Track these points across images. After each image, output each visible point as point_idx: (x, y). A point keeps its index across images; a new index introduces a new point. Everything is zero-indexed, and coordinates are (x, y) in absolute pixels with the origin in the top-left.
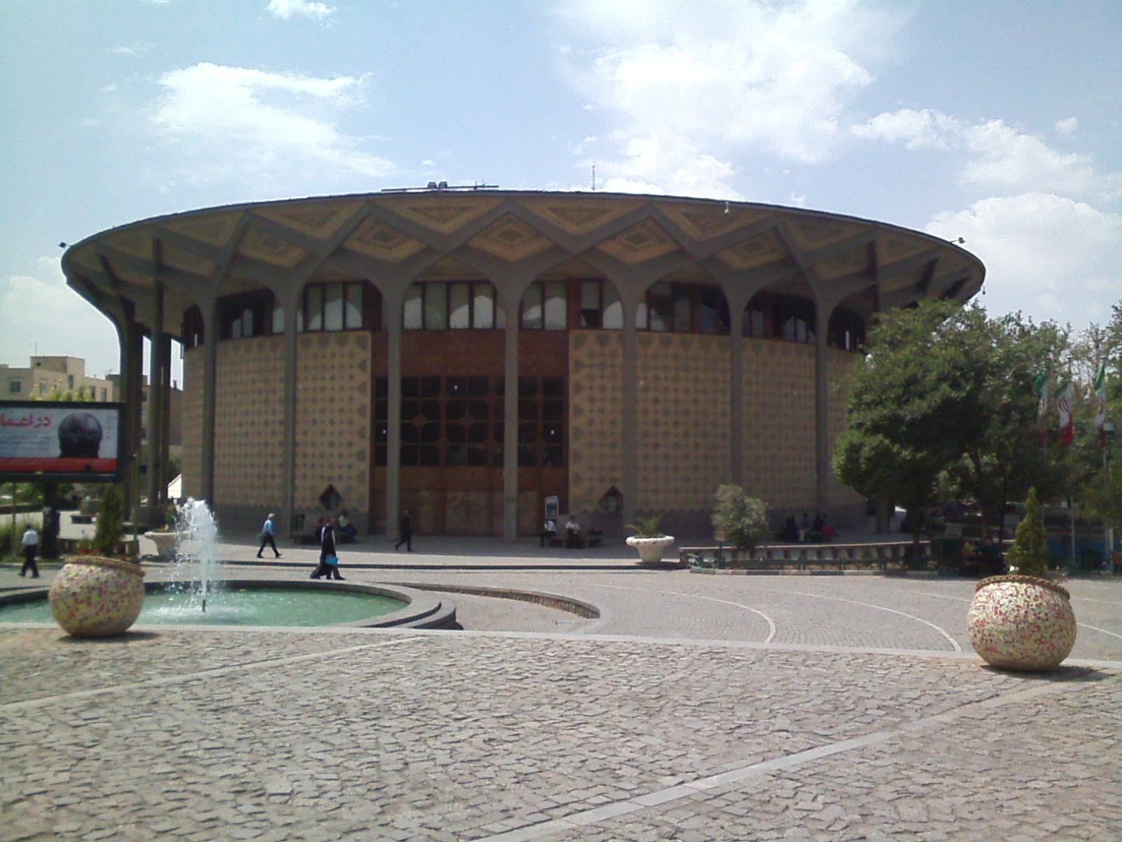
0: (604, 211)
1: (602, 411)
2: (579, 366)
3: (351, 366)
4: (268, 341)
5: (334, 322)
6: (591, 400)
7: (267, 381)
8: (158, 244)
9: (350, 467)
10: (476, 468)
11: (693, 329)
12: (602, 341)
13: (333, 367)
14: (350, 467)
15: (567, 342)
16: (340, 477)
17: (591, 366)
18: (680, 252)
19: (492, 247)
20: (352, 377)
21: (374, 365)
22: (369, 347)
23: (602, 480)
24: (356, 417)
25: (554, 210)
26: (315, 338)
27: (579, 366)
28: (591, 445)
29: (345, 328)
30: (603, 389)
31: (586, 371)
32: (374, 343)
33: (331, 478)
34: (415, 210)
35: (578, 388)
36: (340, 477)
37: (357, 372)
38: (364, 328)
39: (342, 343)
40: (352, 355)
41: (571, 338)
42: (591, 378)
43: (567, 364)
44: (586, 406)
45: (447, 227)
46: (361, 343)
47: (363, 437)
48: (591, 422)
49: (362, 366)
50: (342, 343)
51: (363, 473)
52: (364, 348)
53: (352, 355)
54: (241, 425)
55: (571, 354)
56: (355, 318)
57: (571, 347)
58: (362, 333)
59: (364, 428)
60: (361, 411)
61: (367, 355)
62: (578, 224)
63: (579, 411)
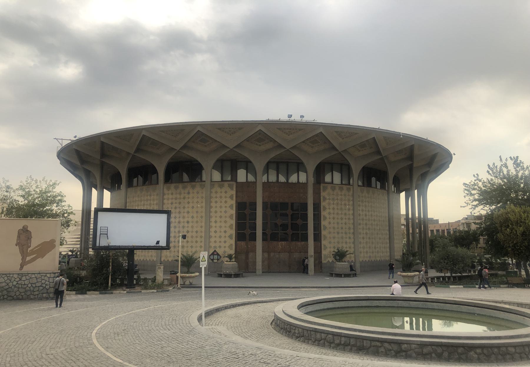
3: (226, 197)
4: (181, 185)
6: (330, 213)
7: (180, 203)
9: (225, 242)
10: (283, 243)
11: (363, 186)
12: (333, 189)
13: (216, 197)
14: (225, 242)
16: (220, 247)
17: (329, 199)
20: (226, 202)
21: (236, 197)
22: (235, 189)
23: (334, 247)
24: (228, 219)
27: (325, 199)
28: (330, 233)
30: (334, 209)
31: (327, 201)
32: (236, 187)
33: (215, 247)
35: (325, 209)
36: (220, 247)
37: (229, 200)
38: (232, 180)
39: (221, 186)
40: (226, 192)
42: (329, 204)
44: (328, 216)
46: (231, 187)
47: (232, 228)
48: (330, 223)
49: (231, 197)
51: (232, 245)
52: (232, 189)
53: (226, 192)
58: (231, 182)
59: (232, 225)
60: (231, 217)
61: (234, 192)
63: (325, 218)
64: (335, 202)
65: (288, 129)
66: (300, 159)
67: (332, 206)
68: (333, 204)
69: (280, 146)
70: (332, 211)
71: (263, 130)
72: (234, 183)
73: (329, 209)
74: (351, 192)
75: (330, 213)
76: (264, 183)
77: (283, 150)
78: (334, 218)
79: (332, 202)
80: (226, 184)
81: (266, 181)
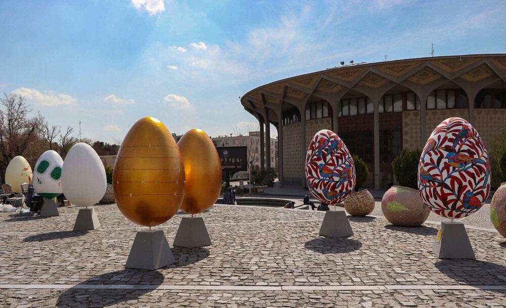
0: (408, 66)
1: (416, 141)
2: (407, 125)
5: (319, 115)
6: (412, 137)
8: (263, 95)
11: (456, 107)
12: (416, 115)
15: (402, 116)
18: (444, 78)
19: (367, 84)
25: (387, 68)
26: (314, 121)
27: (407, 125)
29: (323, 117)
30: (416, 133)
31: (409, 127)
34: (338, 74)
38: (329, 117)
39: (322, 122)
41: (403, 115)
42: (412, 129)
43: (402, 125)
45: (351, 79)
46: (328, 122)
50: (322, 122)
52: (329, 124)
54: (293, 151)
55: (403, 121)
56: (326, 114)
57: (403, 118)
62: (398, 72)
64: (418, 127)
65: (344, 73)
66: (364, 95)
67: (414, 131)
68: (416, 128)
69: (345, 88)
70: (414, 135)
71: (325, 77)
72: (330, 119)
73: (412, 133)
74: (419, 116)
75: (412, 137)
76: (380, 114)
77: (349, 90)
78: (416, 141)
79: (415, 127)
80: (325, 120)
81: (382, 112)
